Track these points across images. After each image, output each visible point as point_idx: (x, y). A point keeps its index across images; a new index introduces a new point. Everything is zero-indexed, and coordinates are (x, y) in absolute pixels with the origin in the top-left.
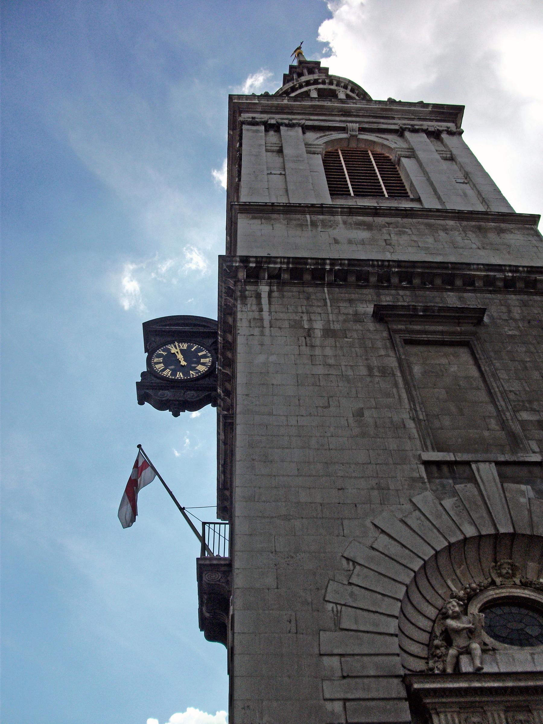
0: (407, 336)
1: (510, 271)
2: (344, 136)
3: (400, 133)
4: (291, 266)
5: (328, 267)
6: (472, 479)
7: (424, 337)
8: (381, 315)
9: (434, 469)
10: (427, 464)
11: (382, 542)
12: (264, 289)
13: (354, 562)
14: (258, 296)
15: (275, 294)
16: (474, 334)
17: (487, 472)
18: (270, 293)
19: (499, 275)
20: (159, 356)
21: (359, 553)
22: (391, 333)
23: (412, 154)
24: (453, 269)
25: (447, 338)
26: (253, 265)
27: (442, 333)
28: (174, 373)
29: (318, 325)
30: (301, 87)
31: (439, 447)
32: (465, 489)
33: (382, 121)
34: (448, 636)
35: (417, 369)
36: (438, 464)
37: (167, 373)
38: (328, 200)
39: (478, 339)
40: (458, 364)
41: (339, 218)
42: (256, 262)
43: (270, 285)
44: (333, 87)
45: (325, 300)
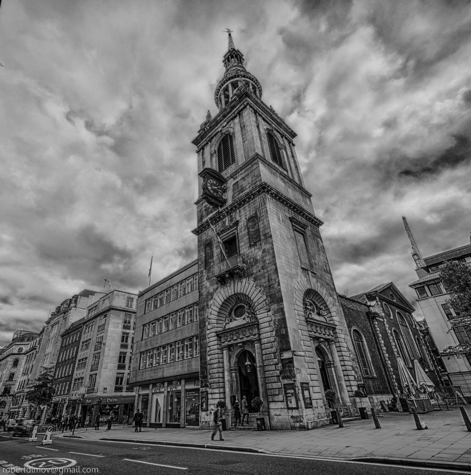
2: (269, 128)
8: (291, 219)
10: (302, 268)
30: (247, 77)
44: (256, 86)
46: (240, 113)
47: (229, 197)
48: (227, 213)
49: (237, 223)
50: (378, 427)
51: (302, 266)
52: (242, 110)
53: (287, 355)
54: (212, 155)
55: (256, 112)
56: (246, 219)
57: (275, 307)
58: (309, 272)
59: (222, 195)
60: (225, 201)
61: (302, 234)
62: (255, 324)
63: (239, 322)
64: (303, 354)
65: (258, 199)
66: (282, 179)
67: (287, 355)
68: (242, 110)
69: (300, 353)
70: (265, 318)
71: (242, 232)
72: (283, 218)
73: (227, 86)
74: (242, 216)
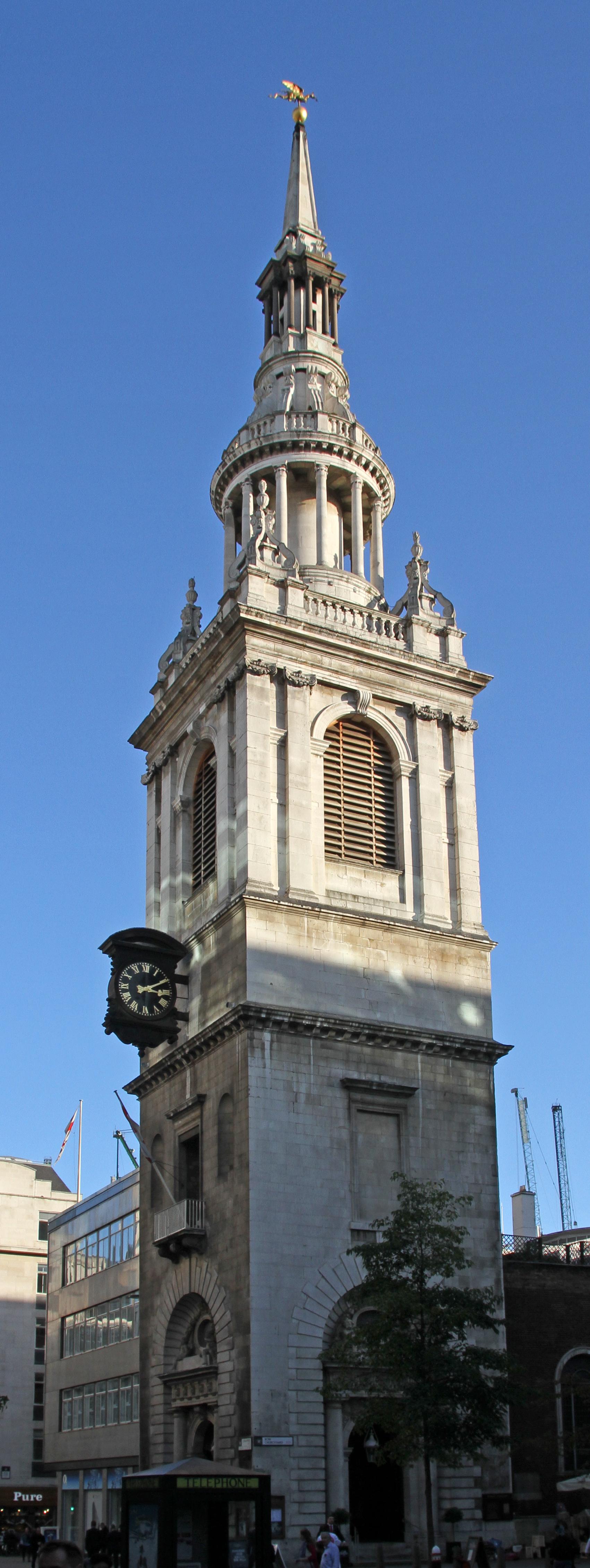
0: (360, 1106)
1: (449, 1041)
4: (291, 1020)
5: (318, 1024)
7: (371, 1108)
9: (356, 1233)
10: (353, 1231)
11: (322, 1284)
12: (267, 1036)
13: (308, 1296)
14: (263, 1049)
15: (275, 1045)
16: (405, 1108)
18: (272, 1042)
19: (440, 1044)
20: (125, 980)
21: (310, 1289)
22: (351, 1101)
24: (409, 1035)
25: (386, 1110)
26: (263, 1016)
27: (384, 1105)
28: (140, 1009)
29: (303, 1089)
33: (398, 680)
35: (360, 1138)
36: (358, 1231)
37: (134, 1006)
39: (406, 1114)
42: (267, 1014)
43: (272, 1032)
44: (350, 466)
45: (310, 1056)
49: (200, 1100)
53: (246, 1444)
54: (175, 816)
56: (217, 1093)
57: (239, 1341)
59: (172, 998)
60: (185, 1017)
61: (397, 1116)
62: (211, 1372)
64: (286, 1441)
65: (239, 1040)
67: (246, 1444)
69: (275, 1440)
70: (226, 1361)
72: (315, 1091)
73: (239, 487)
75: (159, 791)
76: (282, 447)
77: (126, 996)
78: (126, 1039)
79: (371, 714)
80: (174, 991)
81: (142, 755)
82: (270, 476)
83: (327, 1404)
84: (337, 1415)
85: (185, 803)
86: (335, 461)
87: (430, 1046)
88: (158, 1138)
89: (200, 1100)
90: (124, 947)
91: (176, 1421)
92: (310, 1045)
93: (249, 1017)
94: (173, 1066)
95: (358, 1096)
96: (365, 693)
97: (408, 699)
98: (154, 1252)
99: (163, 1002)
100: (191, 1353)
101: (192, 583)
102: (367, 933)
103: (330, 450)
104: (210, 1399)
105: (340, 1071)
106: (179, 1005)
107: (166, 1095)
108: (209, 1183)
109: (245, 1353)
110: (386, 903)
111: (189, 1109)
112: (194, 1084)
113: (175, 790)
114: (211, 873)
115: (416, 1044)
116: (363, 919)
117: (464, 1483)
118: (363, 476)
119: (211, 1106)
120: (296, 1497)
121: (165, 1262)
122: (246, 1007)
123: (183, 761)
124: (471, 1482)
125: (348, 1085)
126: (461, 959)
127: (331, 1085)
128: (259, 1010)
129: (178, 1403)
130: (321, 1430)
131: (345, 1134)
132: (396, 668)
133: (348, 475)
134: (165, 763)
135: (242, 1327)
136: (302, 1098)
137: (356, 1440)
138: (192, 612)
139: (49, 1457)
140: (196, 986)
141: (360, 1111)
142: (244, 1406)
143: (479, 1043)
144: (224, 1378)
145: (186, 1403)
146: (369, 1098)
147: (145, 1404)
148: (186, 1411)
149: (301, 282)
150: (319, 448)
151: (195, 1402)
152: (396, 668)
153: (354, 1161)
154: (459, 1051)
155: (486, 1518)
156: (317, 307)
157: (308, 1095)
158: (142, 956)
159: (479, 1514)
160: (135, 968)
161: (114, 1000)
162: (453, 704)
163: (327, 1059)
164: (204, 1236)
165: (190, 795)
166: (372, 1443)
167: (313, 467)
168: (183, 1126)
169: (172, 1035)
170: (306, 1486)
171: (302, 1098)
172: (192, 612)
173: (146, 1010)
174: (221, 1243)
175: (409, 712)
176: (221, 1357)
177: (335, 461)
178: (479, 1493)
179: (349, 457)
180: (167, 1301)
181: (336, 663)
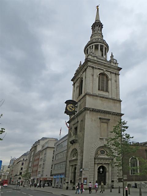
2: (102, 72)
3: (111, 73)
6: (103, 140)
16: (108, 122)
17: (104, 140)
22: (100, 121)
23: (111, 80)
29: (94, 119)
30: (98, 42)
31: (101, 136)
32: (102, 141)
33: (109, 68)
34: (98, 154)
35: (102, 126)
37: (69, 110)
38: (97, 92)
40: (105, 125)
41: (99, 98)
44: (103, 45)
46: (86, 70)
47: (78, 110)
48: (76, 117)
49: (78, 122)
50: (111, 191)
51: (100, 138)
52: (86, 69)
54: (77, 88)
55: (93, 68)
58: (104, 140)
59: (75, 109)
60: (76, 112)
62: (77, 159)
63: (73, 158)
66: (101, 100)
68: (86, 69)
70: (79, 158)
71: (79, 125)
72: (95, 119)
73: (88, 48)
74: (80, 118)
75: (75, 86)
76: (94, 43)
77: (68, 109)
78: (67, 114)
79: (105, 73)
80: (75, 108)
81: (73, 82)
82: (92, 46)
83: (95, 164)
84: (96, 165)
85: (78, 86)
86: (101, 44)
87: (112, 114)
88: (71, 128)
89: (78, 122)
90: (68, 102)
91: (71, 167)
92: (95, 113)
93: (86, 109)
94: (74, 118)
95: (102, 120)
96: (105, 70)
97: (110, 71)
98: (69, 143)
99: (73, 110)
100: (74, 157)
101: (81, 62)
102: (104, 99)
103: (101, 42)
104: (76, 163)
105: (99, 117)
106: (76, 110)
107: (73, 123)
108: (78, 133)
109: (82, 156)
110: (107, 96)
111: (76, 123)
112: (77, 120)
113: (77, 84)
114: (81, 93)
115: (110, 113)
116: (103, 98)
117: (116, 176)
118: (105, 46)
119: (79, 122)
120: (89, 178)
121: (71, 144)
122: (86, 108)
123: (79, 80)
124: (117, 176)
125: (100, 118)
126: (117, 103)
127: (97, 118)
128: (88, 108)
129: (71, 164)
130: (93, 168)
131: (99, 125)
132: (109, 67)
133: (103, 46)
134: (76, 82)
135: (82, 152)
136: (93, 120)
137: (99, 169)
138: (81, 63)
139: (52, 174)
140: (78, 108)
141: (102, 122)
142: (82, 164)
143: (119, 113)
144: (78, 160)
145: (72, 164)
146: (103, 120)
147: (66, 165)
148: (72, 166)
149: (97, 26)
150: (99, 42)
151: (74, 164)
152: (109, 67)
153: (100, 129)
154: (116, 115)
155: (119, 182)
156: (99, 28)
157: (94, 120)
158: (71, 103)
159: (118, 181)
160: (70, 105)
161: (66, 109)
162: (117, 72)
163: (97, 115)
164: (77, 140)
165: (79, 85)
166: (101, 170)
167: (98, 45)
168: (75, 126)
169: (74, 114)
170: (91, 176)
171: (93, 120)
172: (81, 63)
173: (71, 110)
174: (79, 141)
175: (111, 73)
176: (78, 157)
177: (101, 44)
178: (118, 178)
179: (103, 43)
180: (71, 150)
181: (100, 66)
